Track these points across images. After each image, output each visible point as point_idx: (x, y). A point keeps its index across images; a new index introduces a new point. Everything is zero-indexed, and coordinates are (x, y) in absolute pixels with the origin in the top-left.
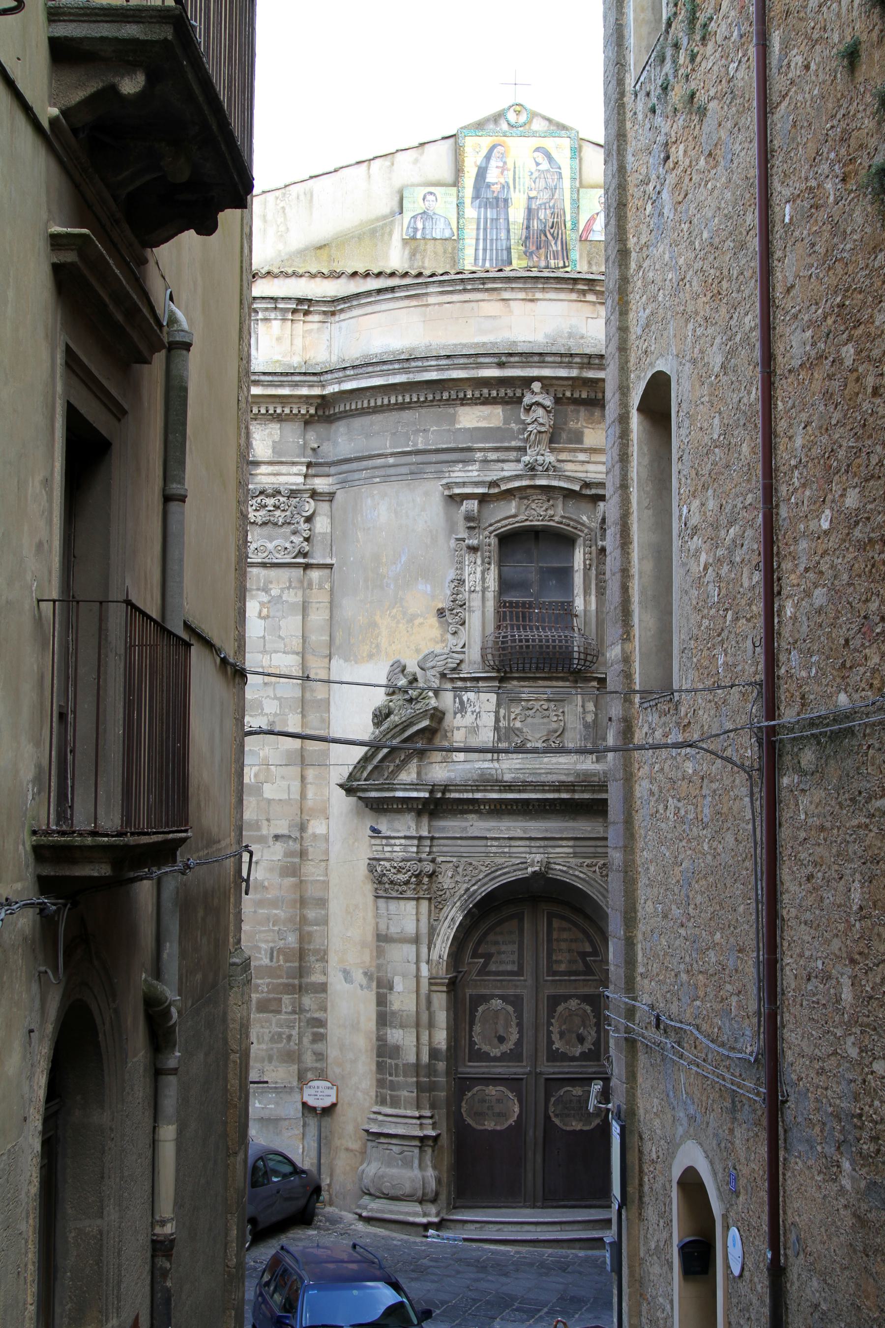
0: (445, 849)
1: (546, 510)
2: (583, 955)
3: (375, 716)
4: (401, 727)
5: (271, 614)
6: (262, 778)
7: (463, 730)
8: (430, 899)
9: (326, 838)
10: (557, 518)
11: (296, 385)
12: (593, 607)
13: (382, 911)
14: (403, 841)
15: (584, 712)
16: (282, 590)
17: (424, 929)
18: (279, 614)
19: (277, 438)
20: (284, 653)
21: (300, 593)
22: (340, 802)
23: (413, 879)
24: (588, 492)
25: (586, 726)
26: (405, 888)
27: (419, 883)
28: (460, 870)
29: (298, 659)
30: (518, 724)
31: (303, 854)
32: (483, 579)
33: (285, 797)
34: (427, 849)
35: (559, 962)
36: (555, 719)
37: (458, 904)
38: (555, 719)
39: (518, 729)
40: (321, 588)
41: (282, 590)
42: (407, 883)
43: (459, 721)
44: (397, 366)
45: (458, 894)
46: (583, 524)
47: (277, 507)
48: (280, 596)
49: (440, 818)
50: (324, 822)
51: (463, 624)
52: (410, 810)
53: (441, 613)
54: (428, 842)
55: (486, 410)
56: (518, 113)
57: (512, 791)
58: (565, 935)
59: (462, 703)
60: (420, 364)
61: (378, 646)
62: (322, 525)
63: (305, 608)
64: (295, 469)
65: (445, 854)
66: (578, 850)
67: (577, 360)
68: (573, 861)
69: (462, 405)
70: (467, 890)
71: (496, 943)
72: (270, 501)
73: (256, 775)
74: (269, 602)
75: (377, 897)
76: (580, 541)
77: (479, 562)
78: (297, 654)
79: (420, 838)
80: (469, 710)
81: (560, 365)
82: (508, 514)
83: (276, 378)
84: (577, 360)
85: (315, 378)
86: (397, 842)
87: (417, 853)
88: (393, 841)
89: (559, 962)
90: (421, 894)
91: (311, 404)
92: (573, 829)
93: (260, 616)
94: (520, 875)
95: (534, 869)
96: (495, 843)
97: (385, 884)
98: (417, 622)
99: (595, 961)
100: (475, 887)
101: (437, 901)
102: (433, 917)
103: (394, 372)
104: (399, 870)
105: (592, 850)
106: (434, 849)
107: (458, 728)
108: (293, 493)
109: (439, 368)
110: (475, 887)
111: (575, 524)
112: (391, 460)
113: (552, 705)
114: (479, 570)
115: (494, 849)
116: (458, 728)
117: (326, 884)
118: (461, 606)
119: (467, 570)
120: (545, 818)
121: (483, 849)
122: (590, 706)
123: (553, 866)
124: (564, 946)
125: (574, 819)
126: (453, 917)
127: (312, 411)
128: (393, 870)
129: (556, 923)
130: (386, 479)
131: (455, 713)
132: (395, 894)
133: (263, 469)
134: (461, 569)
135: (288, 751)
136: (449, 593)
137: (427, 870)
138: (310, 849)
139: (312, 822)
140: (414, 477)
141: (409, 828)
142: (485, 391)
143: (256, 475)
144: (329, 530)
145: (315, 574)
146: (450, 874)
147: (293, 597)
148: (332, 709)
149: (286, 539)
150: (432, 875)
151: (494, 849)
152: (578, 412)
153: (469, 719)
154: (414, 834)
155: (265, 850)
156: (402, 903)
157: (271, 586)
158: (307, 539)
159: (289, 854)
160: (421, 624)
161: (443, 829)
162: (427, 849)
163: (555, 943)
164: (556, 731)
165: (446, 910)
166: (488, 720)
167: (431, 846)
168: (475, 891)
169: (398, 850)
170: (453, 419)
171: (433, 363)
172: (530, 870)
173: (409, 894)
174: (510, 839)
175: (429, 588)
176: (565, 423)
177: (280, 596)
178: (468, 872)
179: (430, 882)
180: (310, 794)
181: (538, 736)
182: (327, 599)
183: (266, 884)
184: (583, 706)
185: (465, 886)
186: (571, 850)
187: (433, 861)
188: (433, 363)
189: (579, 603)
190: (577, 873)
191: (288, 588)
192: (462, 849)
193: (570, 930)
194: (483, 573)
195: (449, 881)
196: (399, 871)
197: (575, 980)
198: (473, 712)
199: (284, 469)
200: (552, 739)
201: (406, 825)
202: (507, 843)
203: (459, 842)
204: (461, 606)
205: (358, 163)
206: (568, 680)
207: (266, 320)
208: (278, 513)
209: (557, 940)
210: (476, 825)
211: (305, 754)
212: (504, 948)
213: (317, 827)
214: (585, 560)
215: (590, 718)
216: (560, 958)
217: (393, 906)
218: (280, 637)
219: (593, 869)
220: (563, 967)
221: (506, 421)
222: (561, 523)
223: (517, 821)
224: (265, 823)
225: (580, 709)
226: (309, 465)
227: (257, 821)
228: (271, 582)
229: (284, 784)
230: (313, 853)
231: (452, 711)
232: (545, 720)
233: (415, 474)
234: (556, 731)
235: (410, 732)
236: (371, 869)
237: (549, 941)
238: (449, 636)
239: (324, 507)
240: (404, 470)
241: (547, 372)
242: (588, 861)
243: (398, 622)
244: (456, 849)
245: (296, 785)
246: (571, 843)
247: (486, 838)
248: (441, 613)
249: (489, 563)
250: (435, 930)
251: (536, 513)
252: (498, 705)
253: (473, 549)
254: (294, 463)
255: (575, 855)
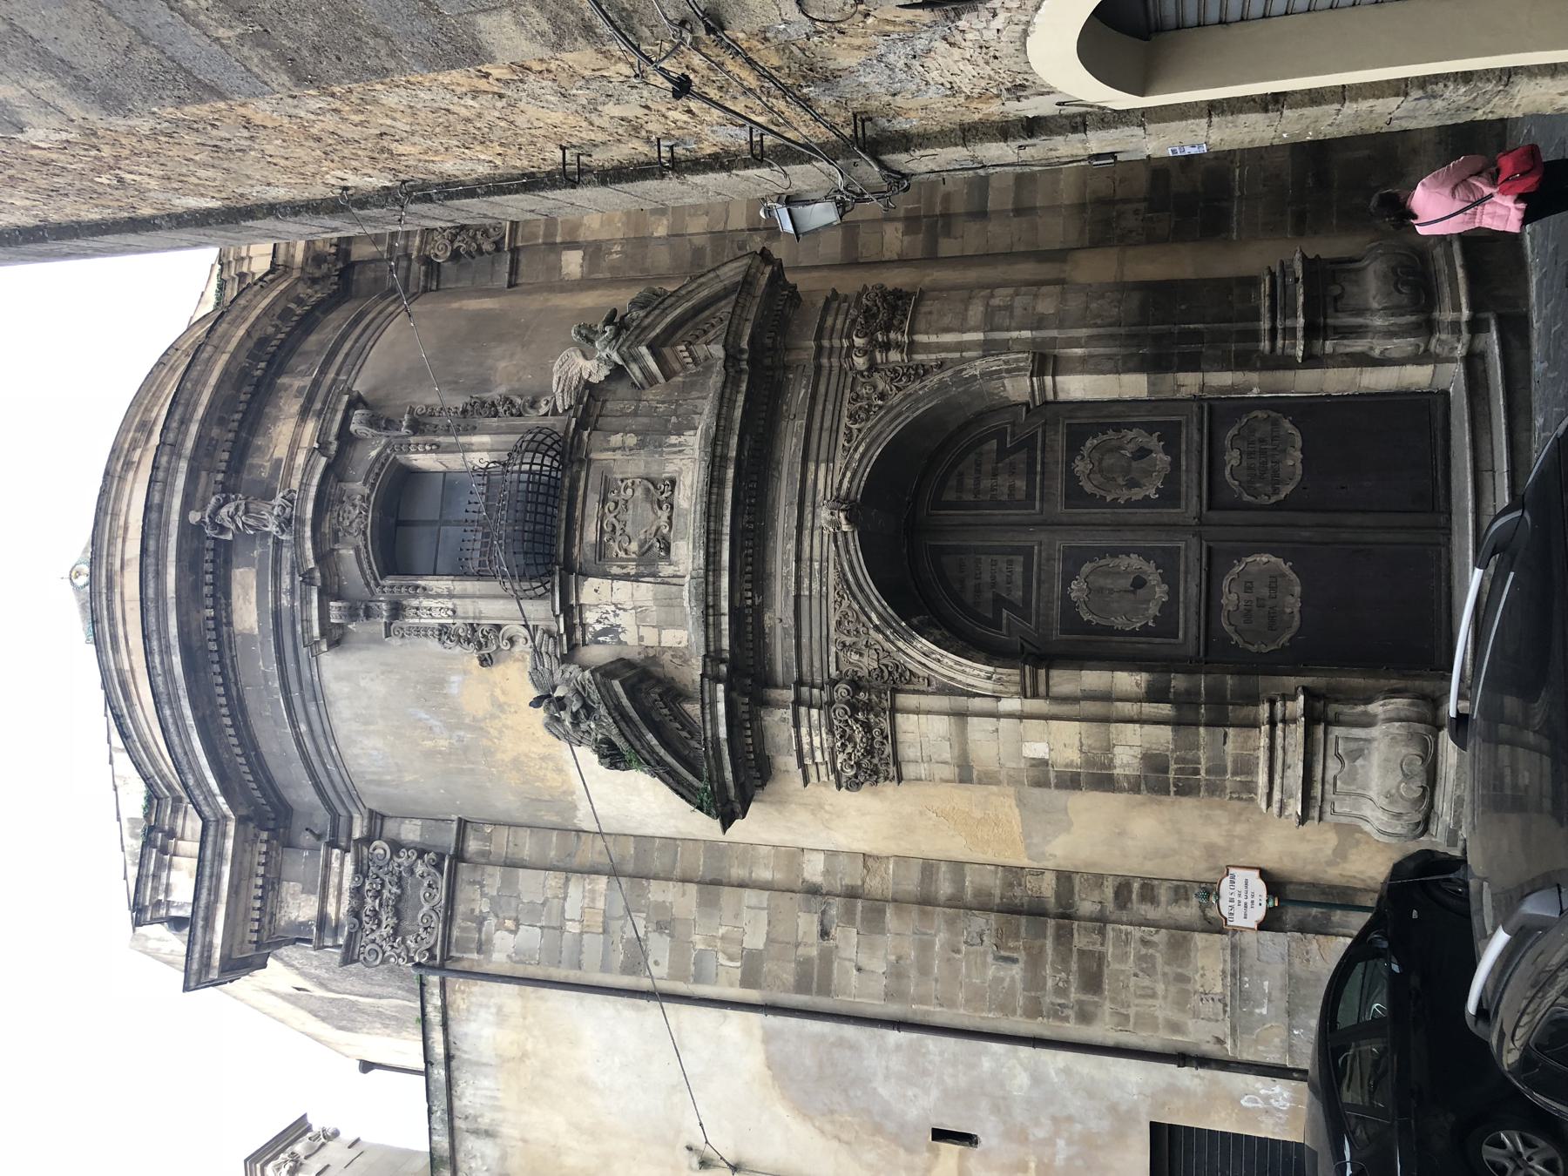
0: (817, 664)
1: (354, 506)
2: (1002, 452)
3: (613, 765)
4: (623, 725)
5: (514, 915)
6: (735, 949)
7: (643, 631)
8: (895, 691)
9: (831, 854)
10: (367, 491)
11: (219, 855)
12: (486, 439)
13: (922, 770)
14: (804, 731)
15: (622, 448)
16: (483, 895)
17: (943, 702)
18: (514, 902)
19: (299, 887)
20: (565, 899)
21: (489, 869)
22: (755, 827)
23: (860, 716)
24: (334, 447)
25: (641, 445)
26: (876, 732)
27: (868, 707)
28: (848, 640)
29: (574, 878)
30: (634, 547)
31: (852, 894)
32: (439, 596)
33: (764, 914)
34: (816, 691)
35: (1012, 488)
36: (629, 491)
37: (900, 644)
38: (629, 491)
39: (641, 547)
40: (489, 838)
41: (483, 895)
42: (868, 728)
43: (629, 637)
44: (167, 712)
45: (887, 645)
46: (379, 455)
47: (378, 894)
48: (492, 899)
49: (772, 671)
50: (807, 856)
51: (498, 627)
52: (755, 718)
53: (485, 661)
54: (805, 690)
55: (236, 591)
56: (79, 574)
57: (718, 553)
58: (969, 482)
59: (605, 632)
60: (160, 680)
61: (544, 758)
62: (410, 832)
63: (512, 864)
64: (335, 864)
65: (828, 660)
66: (823, 456)
67: (164, 460)
68: (840, 463)
69: (230, 624)
70: (876, 628)
71: (978, 590)
72: (370, 904)
73: (731, 958)
74: (497, 916)
75: (900, 779)
76: (401, 458)
77: (415, 603)
78: (567, 880)
79: (798, 702)
80: (613, 620)
81: (167, 486)
82: (353, 558)
83: (206, 883)
84: (164, 460)
85: (211, 831)
86: (805, 740)
87: (820, 708)
88: (806, 747)
89: (1012, 488)
90: (886, 704)
91: (256, 836)
92: (791, 464)
93: (514, 932)
94: (854, 545)
95: (843, 521)
96: (806, 582)
97: (874, 763)
98: (502, 699)
99: (1013, 435)
100: (873, 616)
101: (896, 680)
102: (924, 687)
103: (179, 717)
104: (848, 739)
105: (825, 435)
106: (818, 681)
107: (641, 638)
108: (361, 870)
109: (166, 651)
110: (873, 616)
111: (378, 465)
112: (303, 728)
113: (611, 496)
114: (426, 603)
115: (816, 586)
116: (641, 638)
117: (901, 859)
118: (474, 631)
119: (427, 621)
120: (773, 507)
121: (815, 603)
122: (616, 440)
123: (843, 492)
124: (986, 483)
125: (779, 463)
126: (922, 654)
127: (264, 835)
128: (849, 749)
129: (950, 496)
130: (329, 735)
131: (620, 642)
132: (888, 749)
133: (331, 909)
134: (426, 629)
135: (699, 905)
136: (458, 648)
137: (845, 693)
138: (847, 881)
139: (807, 875)
140: (319, 696)
141: (784, 720)
142: (206, 590)
143: (338, 919)
144: (419, 822)
145: (473, 845)
146: (855, 657)
147: (494, 878)
148: (649, 831)
149: (420, 884)
150: (856, 684)
151: (816, 586)
152: (252, 466)
153: (626, 620)
154: (789, 714)
155: (843, 954)
156: (900, 737)
157: (477, 912)
158: (420, 856)
159: (848, 917)
160: (503, 693)
161: (786, 665)
162: (816, 691)
163: (981, 497)
164: (648, 490)
165: (913, 666)
166: (623, 590)
167: (813, 686)
168: (880, 616)
169: (817, 740)
170: (249, 637)
171: (157, 660)
172: (845, 528)
173: (886, 725)
174: (798, 559)
175: (454, 678)
176: (262, 482)
177: (492, 899)
178: (851, 627)
179: (868, 690)
180: (765, 874)
181: (651, 516)
182: (505, 831)
183: (893, 958)
184: (614, 450)
185: (872, 632)
186: (823, 467)
187: (833, 683)
188: (157, 660)
189: (479, 459)
190: (857, 456)
191: (482, 886)
192: (816, 635)
193: (961, 475)
194: (429, 597)
195: (865, 659)
196: (851, 739)
197: (1043, 463)
198: (616, 615)
199: (334, 880)
200: (657, 495)
201: (778, 722)
202: (805, 565)
203: (805, 640)
204: (474, 631)
205: (111, 762)
206: (579, 473)
207: (167, 891)
208: (386, 893)
209: (977, 492)
210: (779, 613)
211: (708, 879)
212: (986, 577)
213: (814, 869)
214: (425, 452)
215: (632, 440)
216: (1006, 490)
217: (908, 752)
218: (543, 904)
219: (855, 432)
220: (1021, 484)
221: (249, 564)
222: (373, 485)
223: (775, 549)
224: (801, 951)
225: (618, 455)
226: (333, 844)
227: (799, 963)
228: (473, 910)
229: (746, 915)
230: (851, 875)
231: (619, 648)
232: (630, 506)
233: (317, 694)
234: (648, 490)
235: (635, 713)
236: (854, 785)
237: (977, 505)
238: (517, 649)
239: (390, 827)
240: (312, 708)
241: (177, 502)
242: (842, 440)
243: (505, 726)
244: (816, 646)
245: (750, 897)
246: (812, 467)
247: (798, 597)
248: (485, 661)
249: (417, 587)
250: (945, 685)
251: (357, 516)
252: (605, 575)
253: (397, 610)
254: (327, 865)
255: (830, 460)
